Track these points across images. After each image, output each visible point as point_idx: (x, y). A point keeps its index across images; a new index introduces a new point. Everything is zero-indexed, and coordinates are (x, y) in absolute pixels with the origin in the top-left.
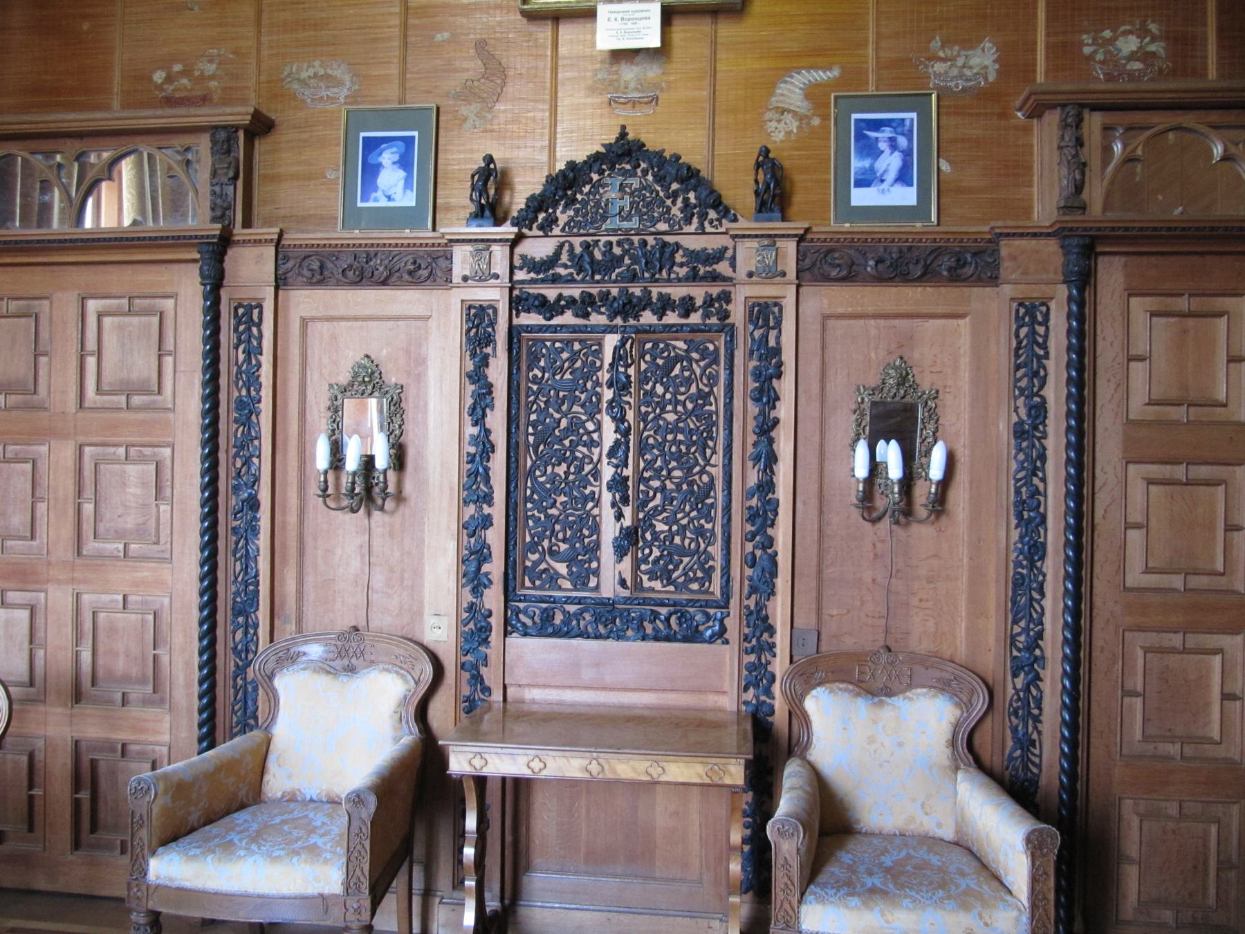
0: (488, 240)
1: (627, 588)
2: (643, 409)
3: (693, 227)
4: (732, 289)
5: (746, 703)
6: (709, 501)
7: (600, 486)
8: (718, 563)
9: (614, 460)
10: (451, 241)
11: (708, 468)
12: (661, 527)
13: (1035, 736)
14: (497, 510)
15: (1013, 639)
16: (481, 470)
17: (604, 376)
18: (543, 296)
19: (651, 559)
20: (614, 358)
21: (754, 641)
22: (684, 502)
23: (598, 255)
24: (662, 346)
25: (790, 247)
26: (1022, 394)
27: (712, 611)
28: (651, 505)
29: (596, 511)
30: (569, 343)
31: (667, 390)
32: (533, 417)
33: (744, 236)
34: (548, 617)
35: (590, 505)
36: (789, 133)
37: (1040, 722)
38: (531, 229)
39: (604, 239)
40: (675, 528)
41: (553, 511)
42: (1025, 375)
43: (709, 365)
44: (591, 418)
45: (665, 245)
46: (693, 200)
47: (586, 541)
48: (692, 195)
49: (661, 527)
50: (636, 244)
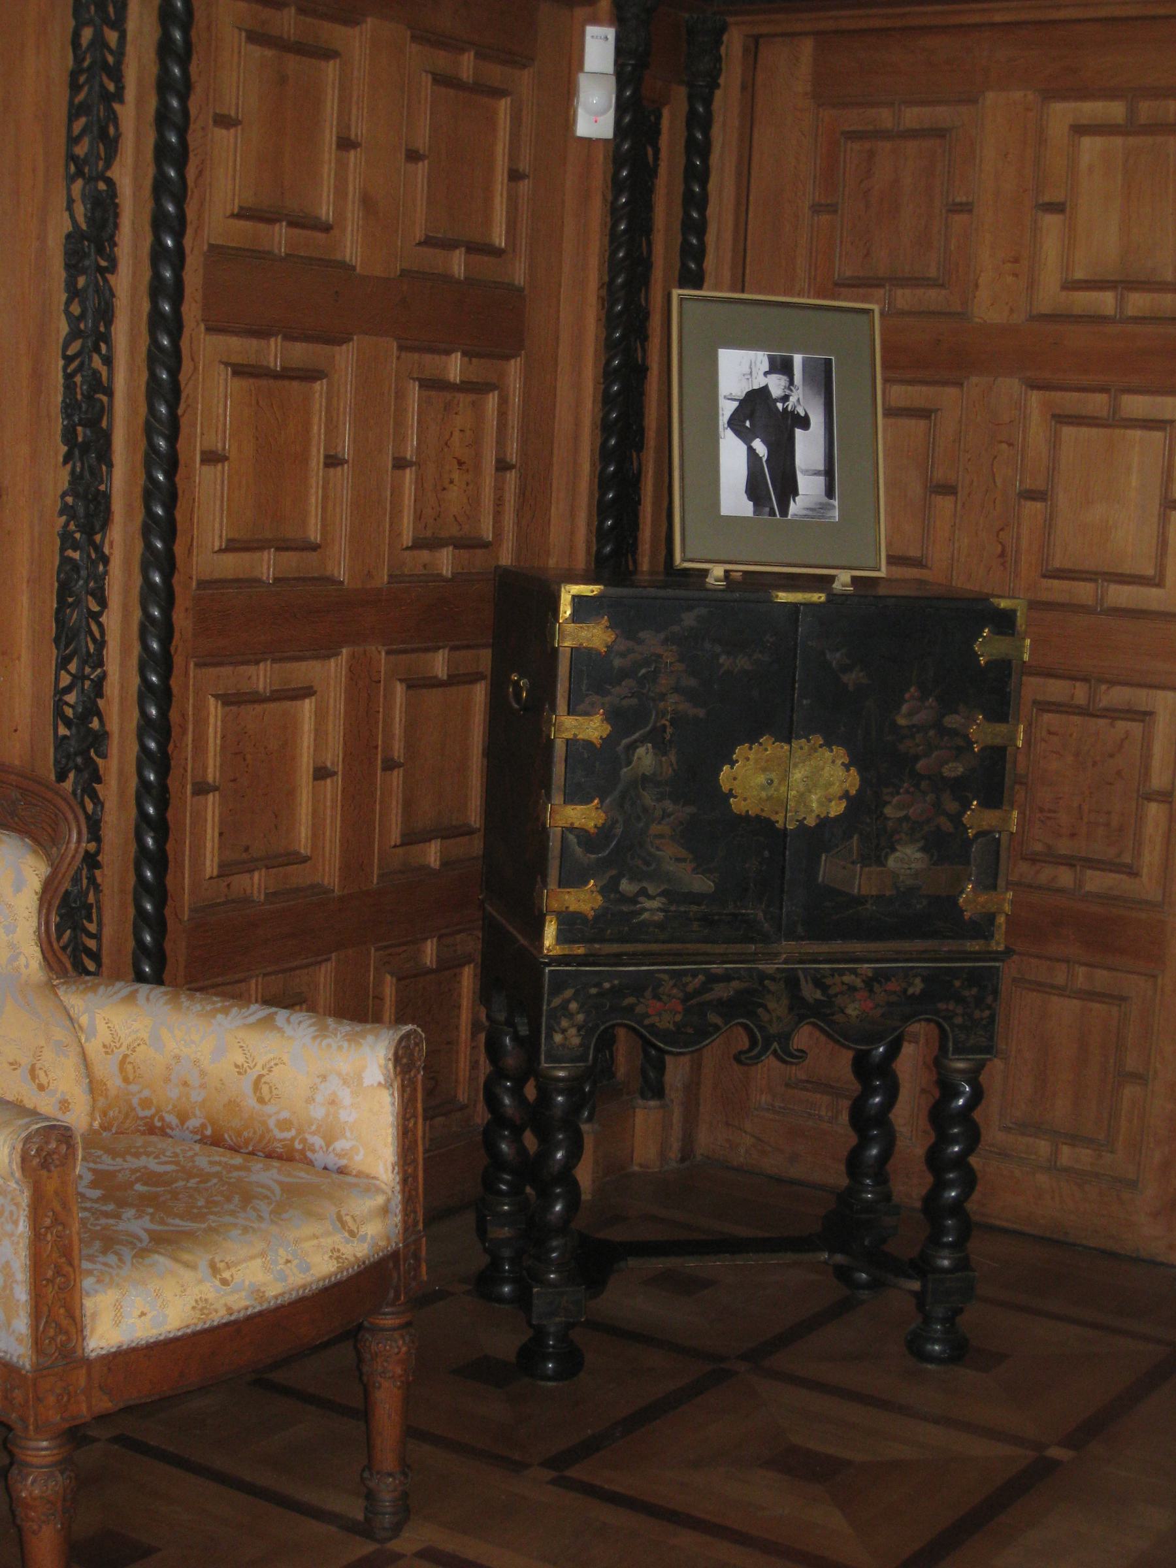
26: (80, 173)
42: (84, 132)
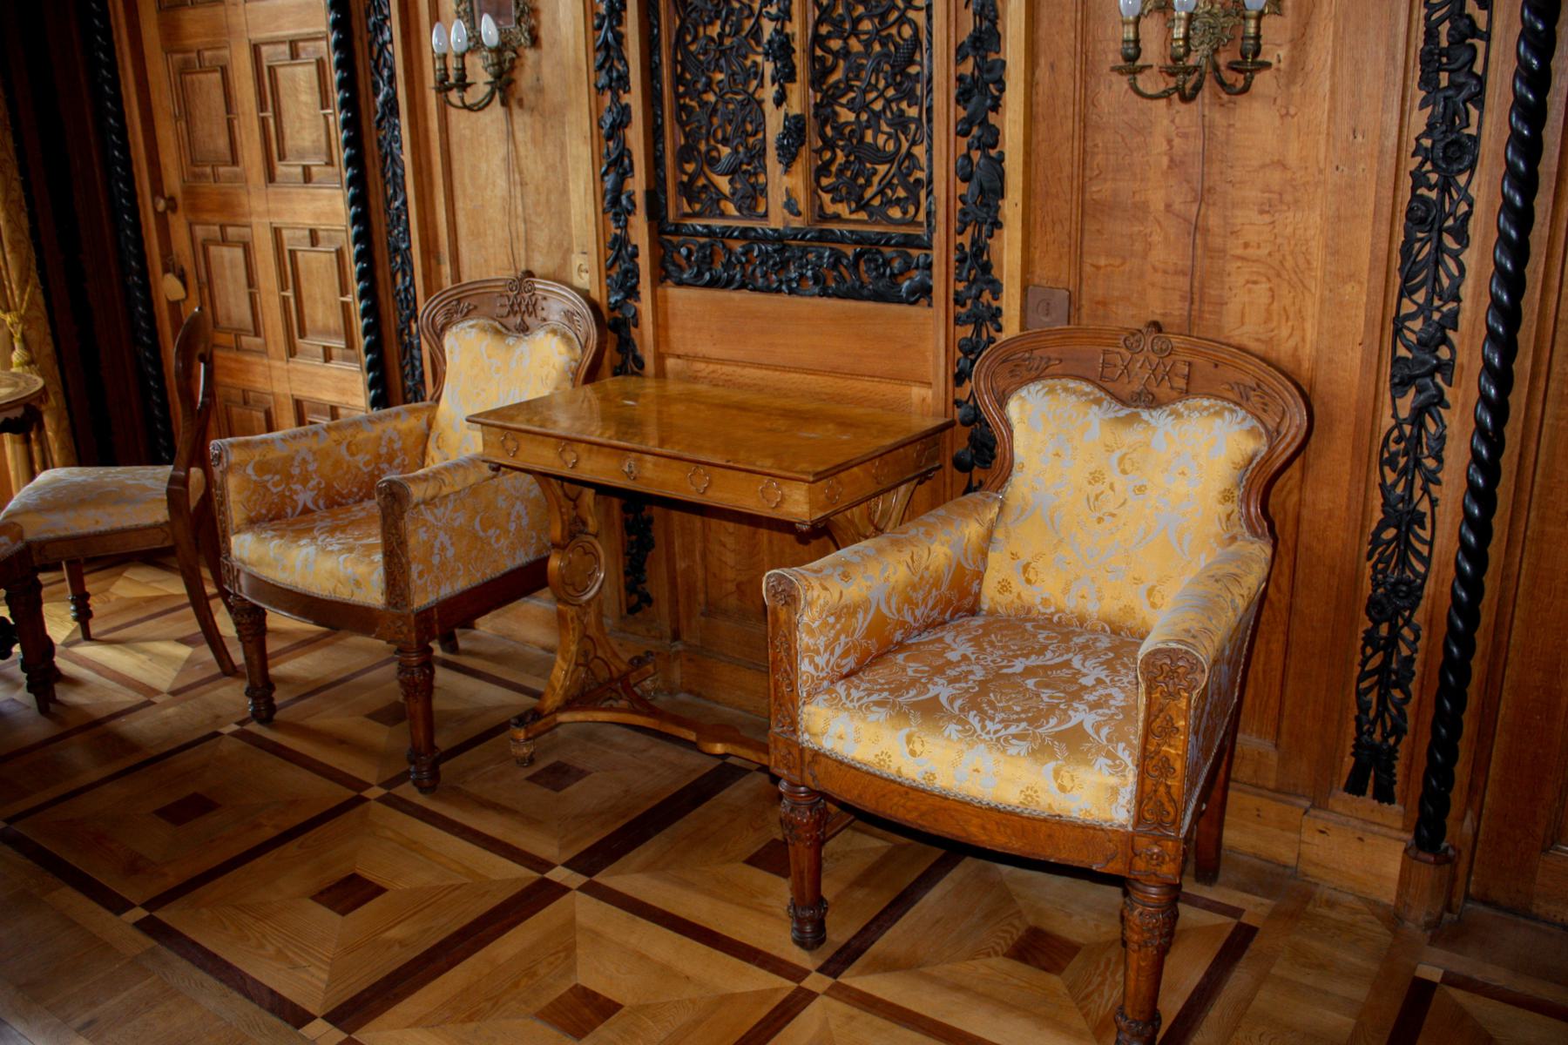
1: (799, 214)
5: (957, 403)
6: (913, 70)
11: (911, 14)
12: (846, 116)
13: (1424, 506)
14: (634, 99)
15: (1399, 324)
19: (834, 169)
22: (877, 70)
37: (1438, 482)
40: (864, 117)
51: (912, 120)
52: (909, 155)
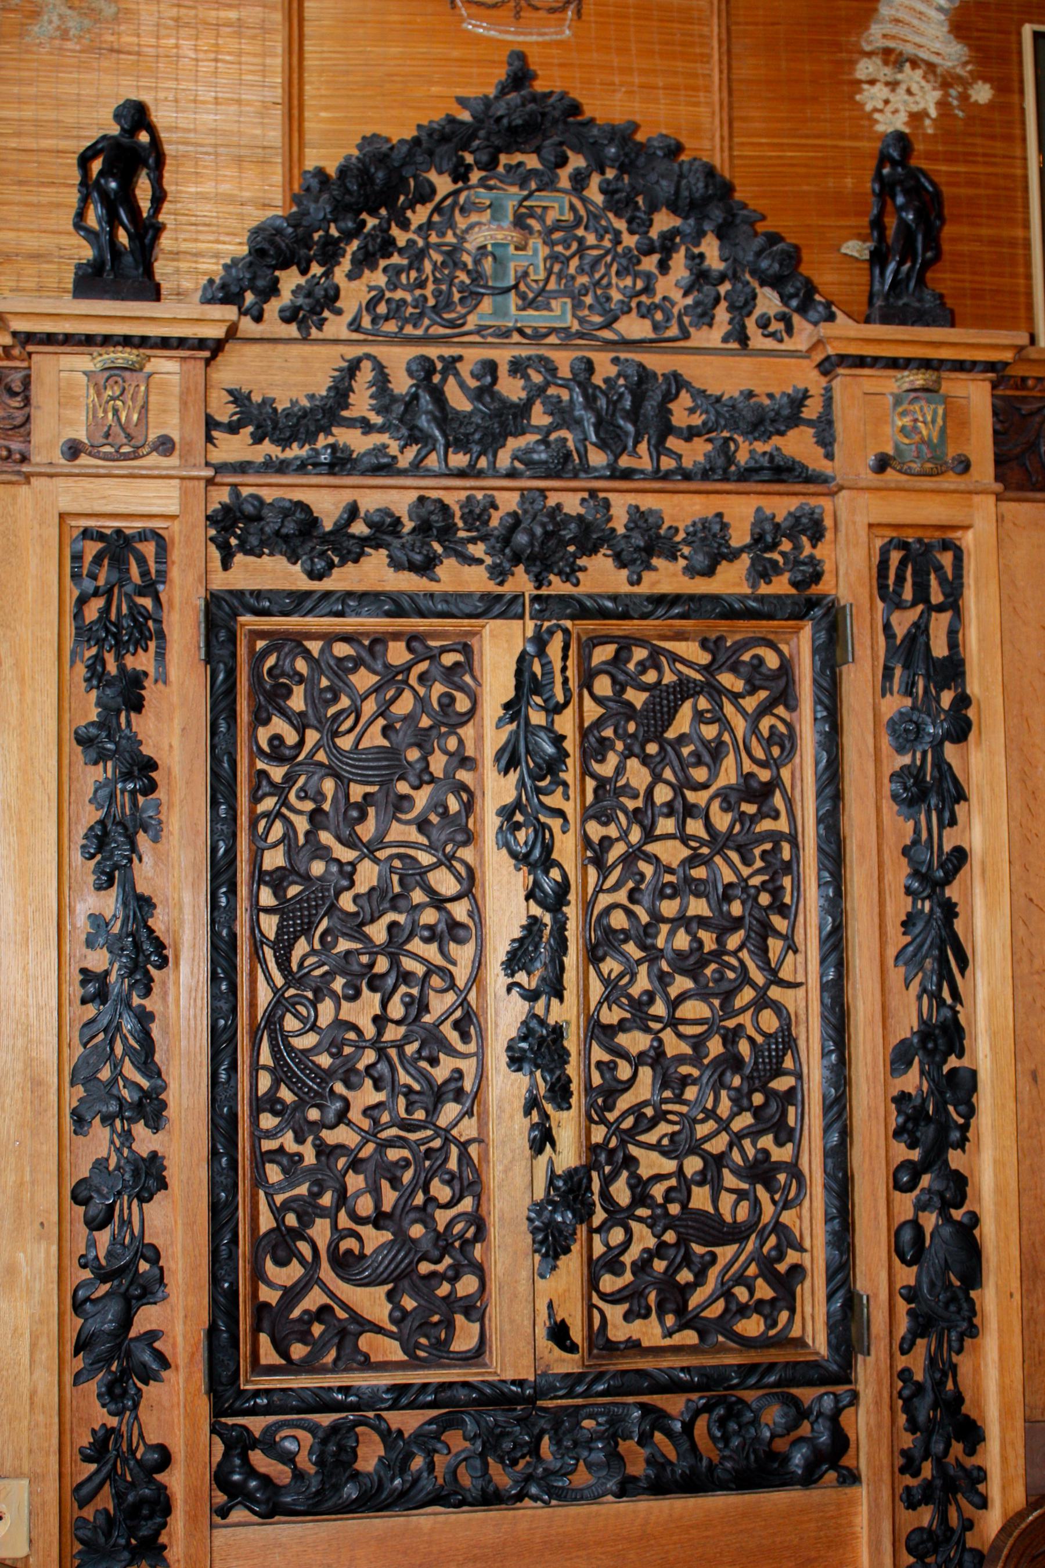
0: (144, 342)
2: (595, 831)
3: (713, 336)
4: (826, 503)
7: (480, 1056)
8: (815, 1256)
9: (521, 977)
10: (29, 338)
14: (182, 1141)
16: (128, 1024)
17: (489, 735)
18: (303, 507)
19: (628, 1258)
20: (518, 687)
21: (927, 1470)
23: (459, 401)
24: (640, 654)
25: (976, 396)
27: (806, 1395)
28: (624, 1102)
29: (467, 1129)
30: (379, 641)
31: (657, 778)
32: (274, 859)
33: (861, 362)
34: (336, 1454)
35: (450, 1111)
36: (917, 117)
38: (258, 318)
39: (473, 356)
41: (341, 1135)
43: (765, 709)
44: (447, 861)
45: (645, 375)
46: (714, 261)
47: (442, 1217)
48: (711, 249)
49: (651, 1163)
50: (565, 372)
51: (779, 1166)
52: (778, 1227)
